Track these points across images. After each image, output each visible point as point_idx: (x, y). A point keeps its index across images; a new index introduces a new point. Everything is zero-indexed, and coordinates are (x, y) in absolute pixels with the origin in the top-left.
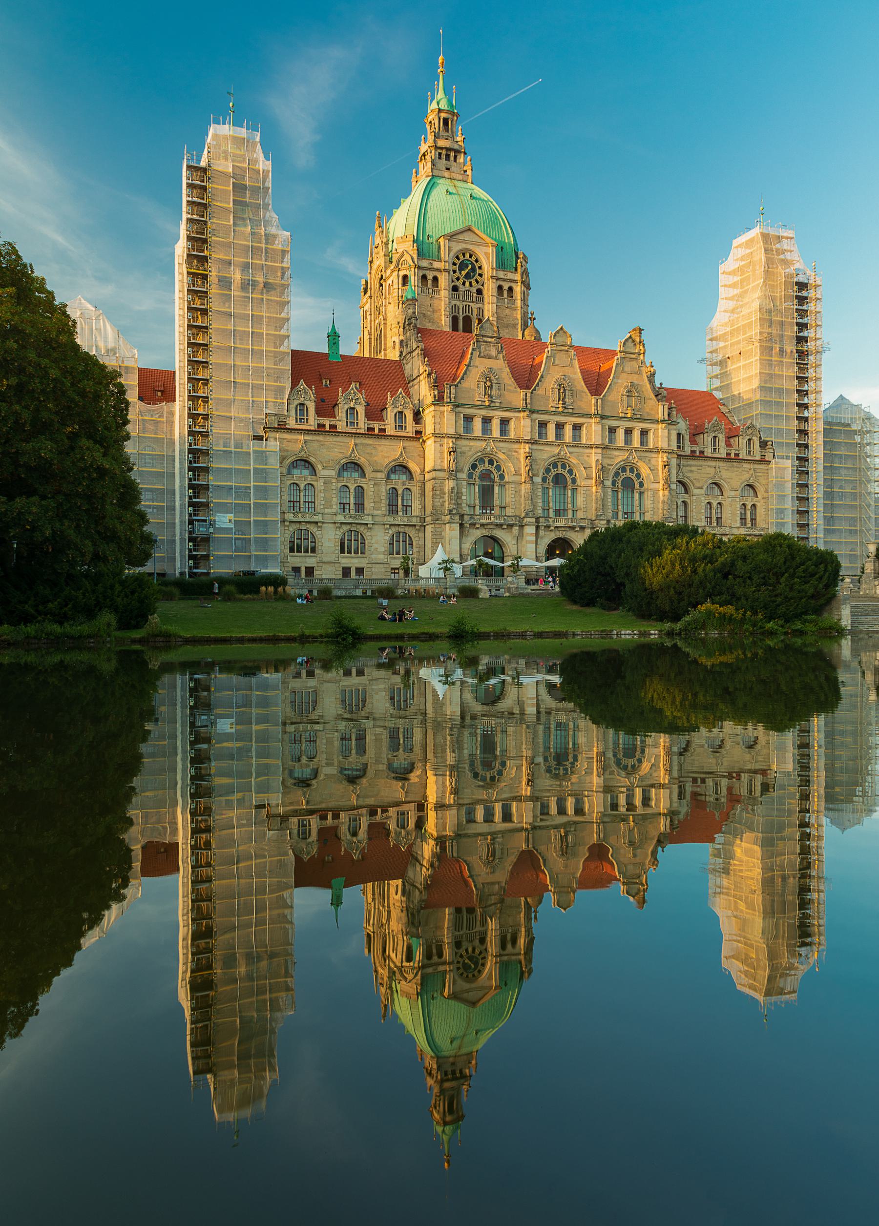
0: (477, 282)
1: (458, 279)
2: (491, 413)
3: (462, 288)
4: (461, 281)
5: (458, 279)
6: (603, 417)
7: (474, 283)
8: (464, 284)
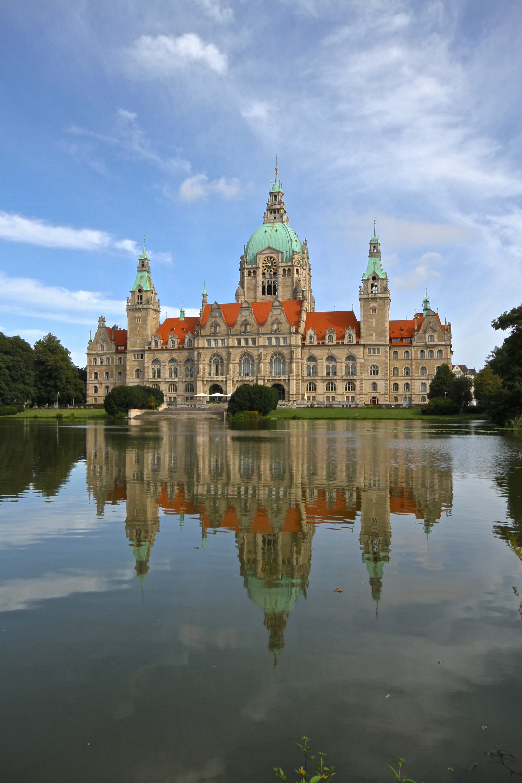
0: (274, 269)
1: (265, 270)
2: (217, 338)
3: (267, 273)
4: (266, 270)
5: (265, 270)
6: (263, 334)
7: (272, 270)
8: (268, 271)
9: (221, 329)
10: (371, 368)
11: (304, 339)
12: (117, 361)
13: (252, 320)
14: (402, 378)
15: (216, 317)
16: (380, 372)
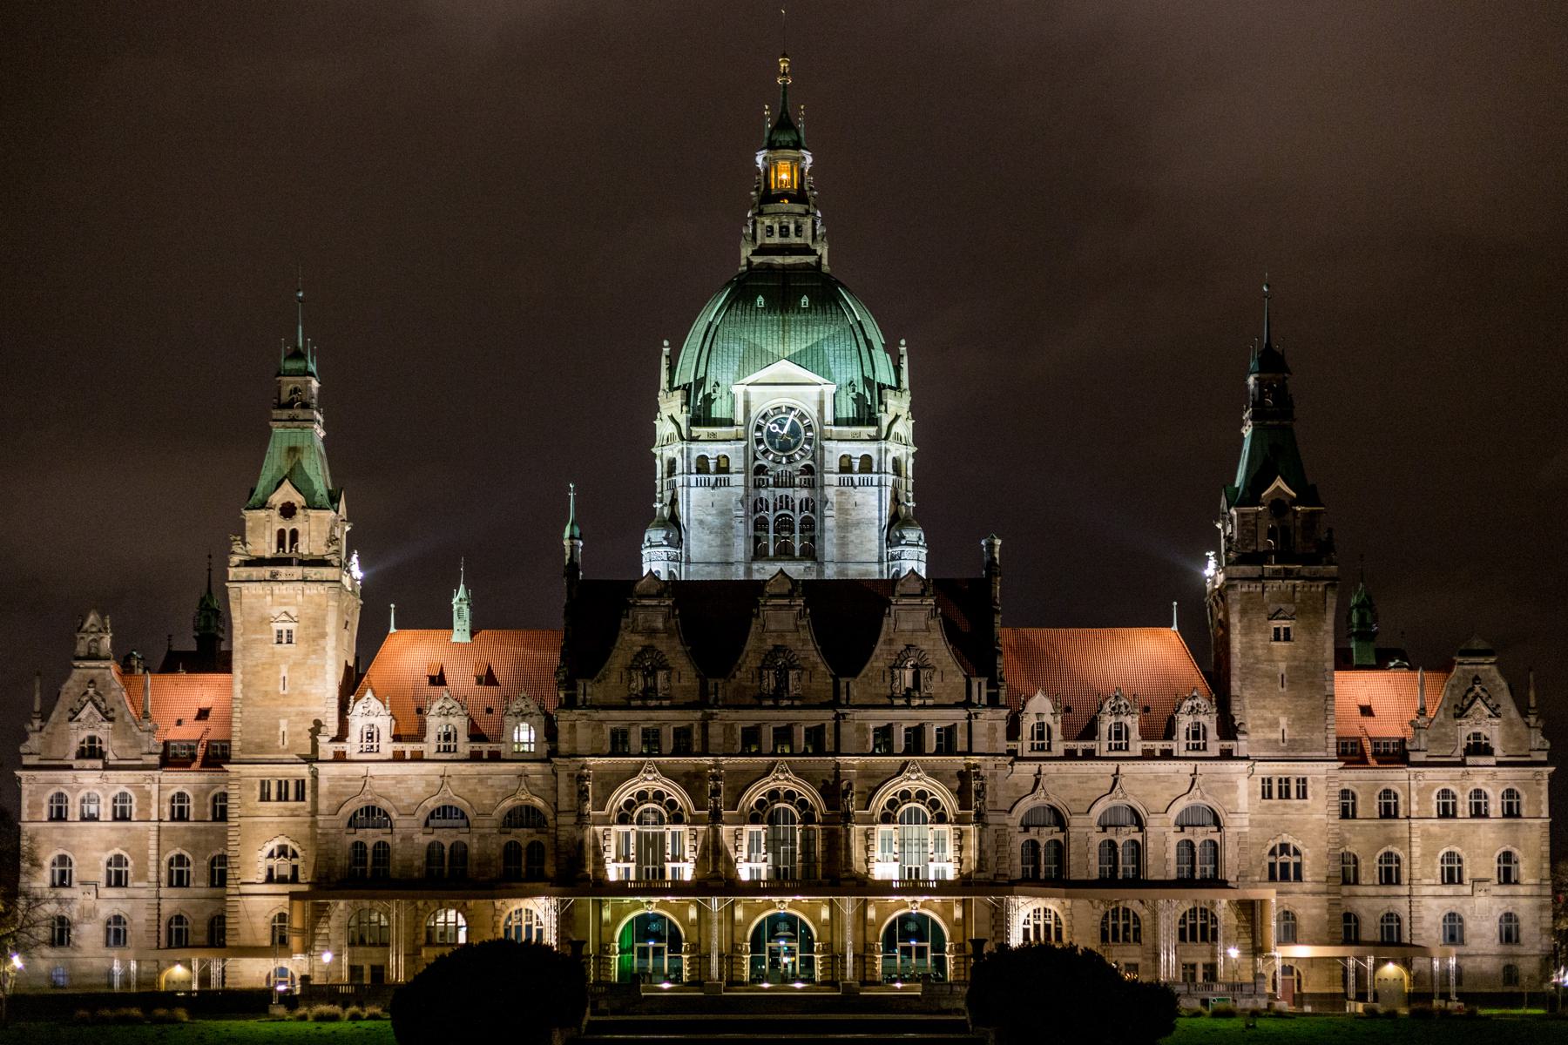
9: (675, 683)
10: (1273, 852)
11: (1013, 732)
12: (167, 809)
13: (808, 650)
14: (1372, 891)
15: (652, 632)
16: (1307, 874)
